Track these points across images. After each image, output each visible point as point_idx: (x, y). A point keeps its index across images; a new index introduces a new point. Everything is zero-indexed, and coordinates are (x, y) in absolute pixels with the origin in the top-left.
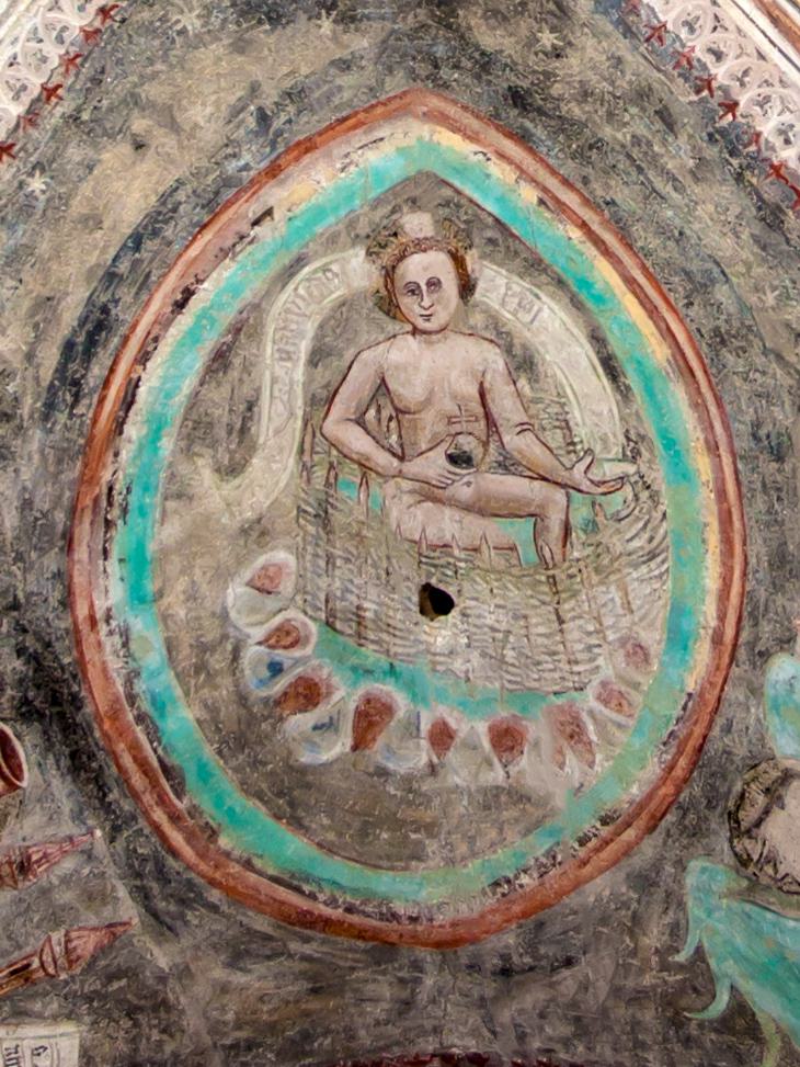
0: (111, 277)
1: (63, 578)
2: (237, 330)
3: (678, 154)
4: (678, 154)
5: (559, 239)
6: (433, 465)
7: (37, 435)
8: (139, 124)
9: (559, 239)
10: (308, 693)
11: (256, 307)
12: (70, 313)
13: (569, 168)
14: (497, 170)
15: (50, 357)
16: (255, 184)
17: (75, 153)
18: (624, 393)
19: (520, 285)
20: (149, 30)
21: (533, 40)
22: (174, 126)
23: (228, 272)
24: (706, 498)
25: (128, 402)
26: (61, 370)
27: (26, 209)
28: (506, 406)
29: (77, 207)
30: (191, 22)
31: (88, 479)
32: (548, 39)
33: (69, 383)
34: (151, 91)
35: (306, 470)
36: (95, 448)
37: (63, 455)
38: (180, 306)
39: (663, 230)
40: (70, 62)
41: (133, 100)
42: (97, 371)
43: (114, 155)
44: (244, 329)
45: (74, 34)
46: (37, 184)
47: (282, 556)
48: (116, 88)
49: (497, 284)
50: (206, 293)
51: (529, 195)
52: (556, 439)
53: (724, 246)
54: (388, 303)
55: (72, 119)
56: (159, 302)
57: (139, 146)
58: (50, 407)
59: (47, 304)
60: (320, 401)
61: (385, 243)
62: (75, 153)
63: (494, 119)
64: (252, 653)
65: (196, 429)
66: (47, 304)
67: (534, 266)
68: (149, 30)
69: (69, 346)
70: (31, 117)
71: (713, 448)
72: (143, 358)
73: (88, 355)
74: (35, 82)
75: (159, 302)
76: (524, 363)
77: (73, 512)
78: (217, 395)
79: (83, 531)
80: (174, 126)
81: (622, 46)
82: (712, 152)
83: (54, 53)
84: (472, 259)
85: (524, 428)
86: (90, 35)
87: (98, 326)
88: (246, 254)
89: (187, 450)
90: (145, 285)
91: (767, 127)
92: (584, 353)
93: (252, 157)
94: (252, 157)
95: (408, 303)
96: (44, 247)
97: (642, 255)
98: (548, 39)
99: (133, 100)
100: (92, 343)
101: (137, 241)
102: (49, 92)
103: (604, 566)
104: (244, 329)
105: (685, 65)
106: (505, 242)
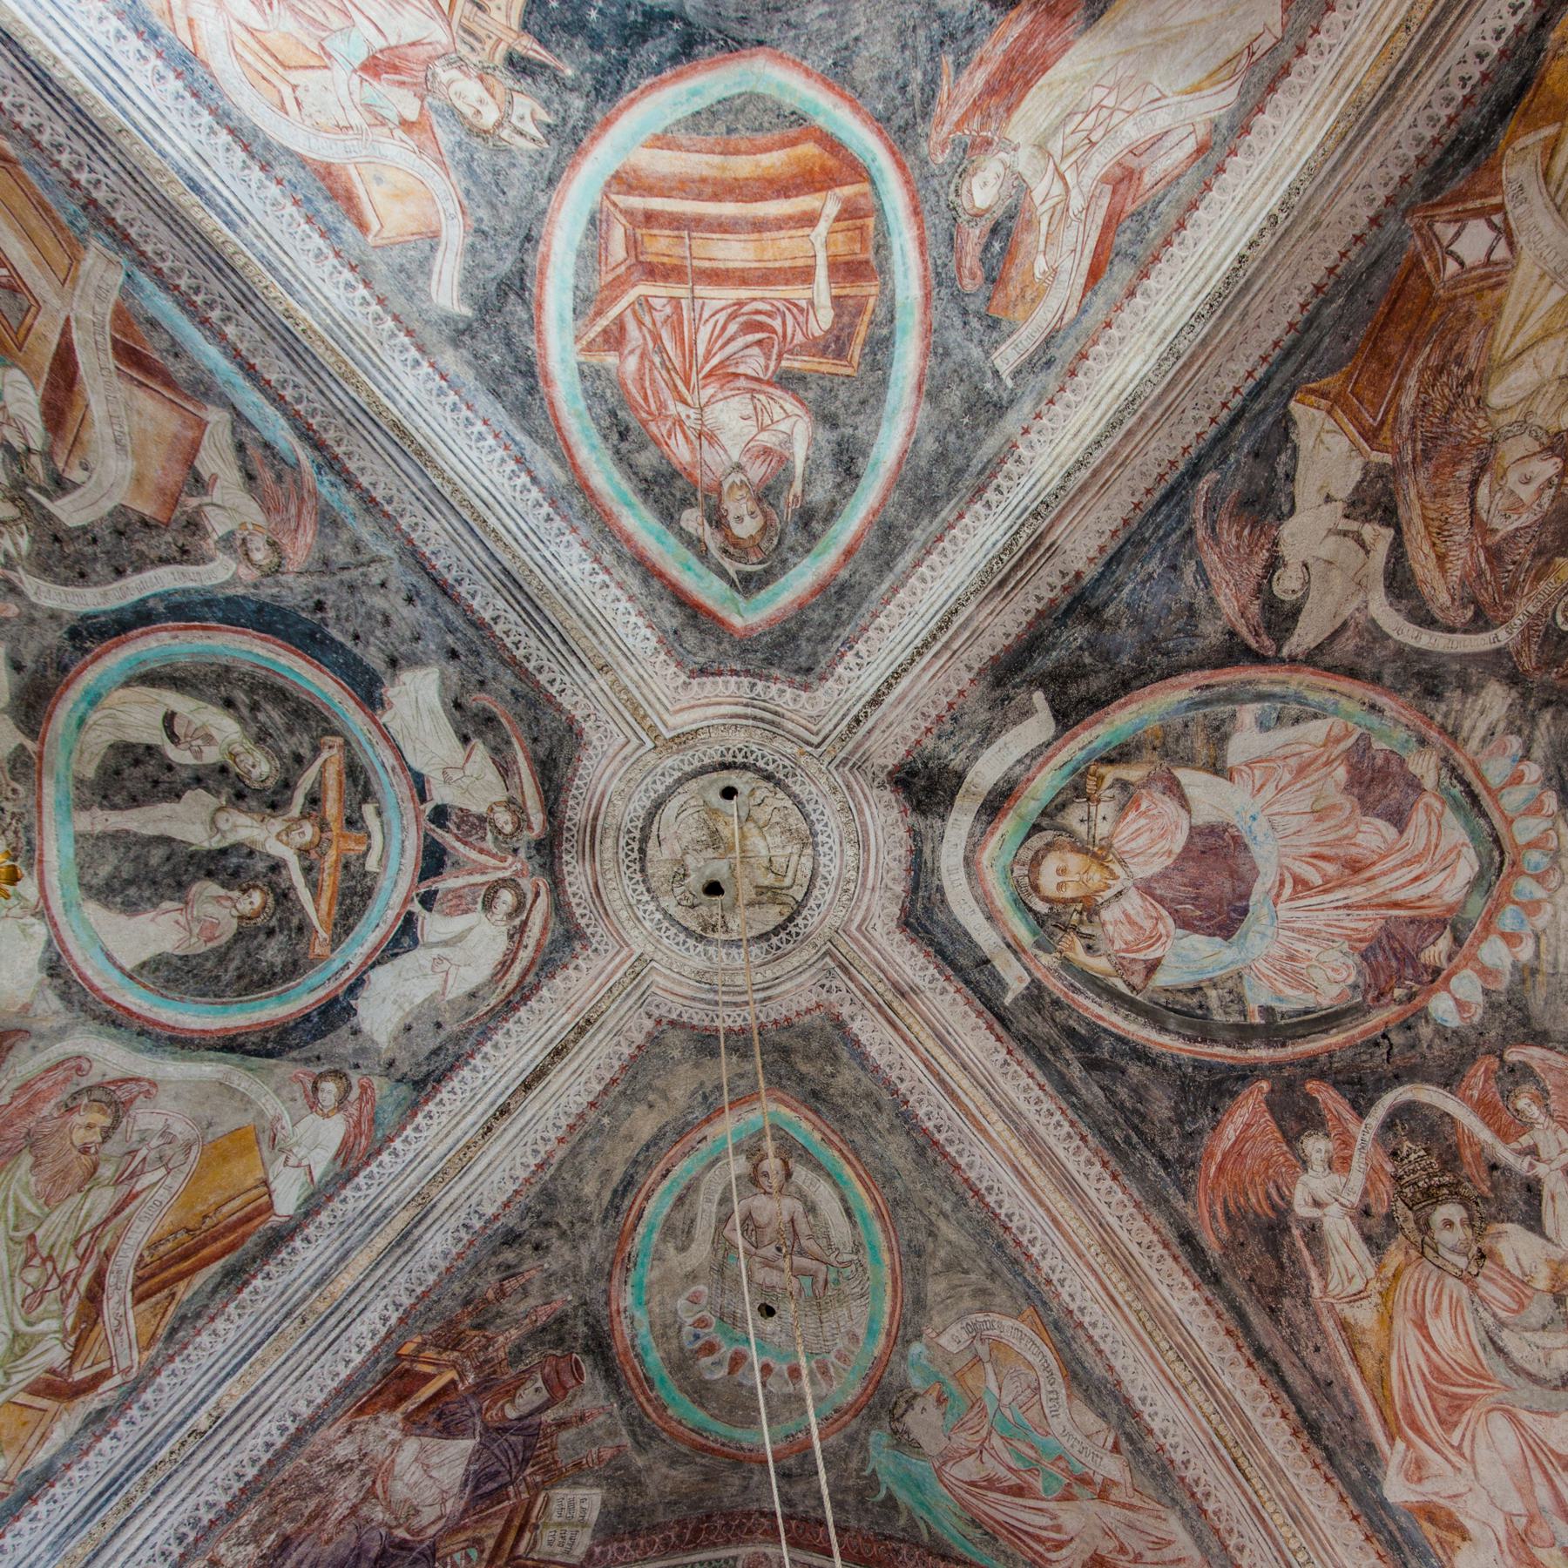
0: (635, 1162)
1: (606, 1292)
2: (688, 1188)
3: (882, 1122)
4: (882, 1122)
5: (829, 1156)
6: (770, 1251)
7: (599, 1229)
8: (651, 1097)
9: (829, 1156)
10: (710, 1348)
11: (697, 1179)
12: (617, 1176)
13: (836, 1126)
14: (805, 1125)
15: (607, 1196)
16: (700, 1125)
17: (623, 1108)
18: (854, 1225)
19: (811, 1175)
20: (658, 1056)
21: (822, 1070)
22: (666, 1099)
23: (686, 1163)
24: (887, 1271)
25: (640, 1217)
26: (611, 1202)
27: (601, 1131)
28: (802, 1227)
29: (623, 1131)
30: (676, 1054)
31: (620, 1249)
32: (829, 1069)
33: (614, 1208)
34: (657, 1083)
35: (715, 1250)
36: (623, 1237)
37: (610, 1239)
38: (664, 1176)
39: (874, 1155)
40: (623, 1068)
41: (649, 1086)
42: (627, 1203)
43: (640, 1109)
44: (691, 1188)
45: (626, 1057)
46: (606, 1120)
47: (702, 1287)
48: (643, 1080)
49: (801, 1173)
50: (676, 1171)
51: (817, 1136)
52: (824, 1243)
53: (900, 1163)
54: (754, 1179)
55: (623, 1093)
56: (655, 1174)
57: (651, 1106)
58: (606, 1218)
59: (607, 1172)
60: (724, 1220)
61: (754, 1153)
62: (623, 1108)
63: (804, 1102)
64: (687, 1329)
65: (669, 1230)
66: (607, 1172)
67: (818, 1167)
68: (658, 1056)
69: (615, 1192)
70: (605, 1092)
71: (891, 1250)
72: (647, 1198)
73: (623, 1196)
74: (608, 1076)
75: (655, 1174)
76: (811, 1209)
77: (613, 1264)
78: (678, 1217)
79: (617, 1272)
80: (666, 1099)
81: (861, 1074)
82: (897, 1122)
83: (617, 1064)
84: (791, 1162)
85: (810, 1237)
86: (633, 1057)
87: (628, 1183)
88: (695, 1156)
89: (664, 1241)
90: (650, 1167)
91: (921, 1112)
92: (837, 1206)
93: (699, 1113)
94: (699, 1113)
95: (762, 1180)
96: (607, 1148)
97: (865, 1165)
98: (829, 1069)
99: (649, 1086)
100: (625, 1190)
101: (647, 1147)
102: (614, 1081)
103: (841, 1299)
104: (691, 1188)
105: (887, 1083)
106: (806, 1156)
